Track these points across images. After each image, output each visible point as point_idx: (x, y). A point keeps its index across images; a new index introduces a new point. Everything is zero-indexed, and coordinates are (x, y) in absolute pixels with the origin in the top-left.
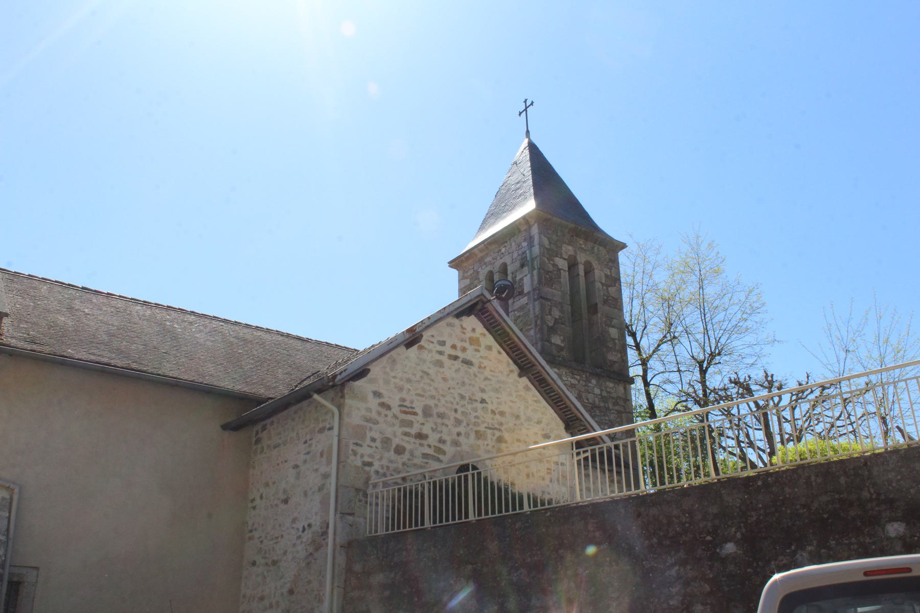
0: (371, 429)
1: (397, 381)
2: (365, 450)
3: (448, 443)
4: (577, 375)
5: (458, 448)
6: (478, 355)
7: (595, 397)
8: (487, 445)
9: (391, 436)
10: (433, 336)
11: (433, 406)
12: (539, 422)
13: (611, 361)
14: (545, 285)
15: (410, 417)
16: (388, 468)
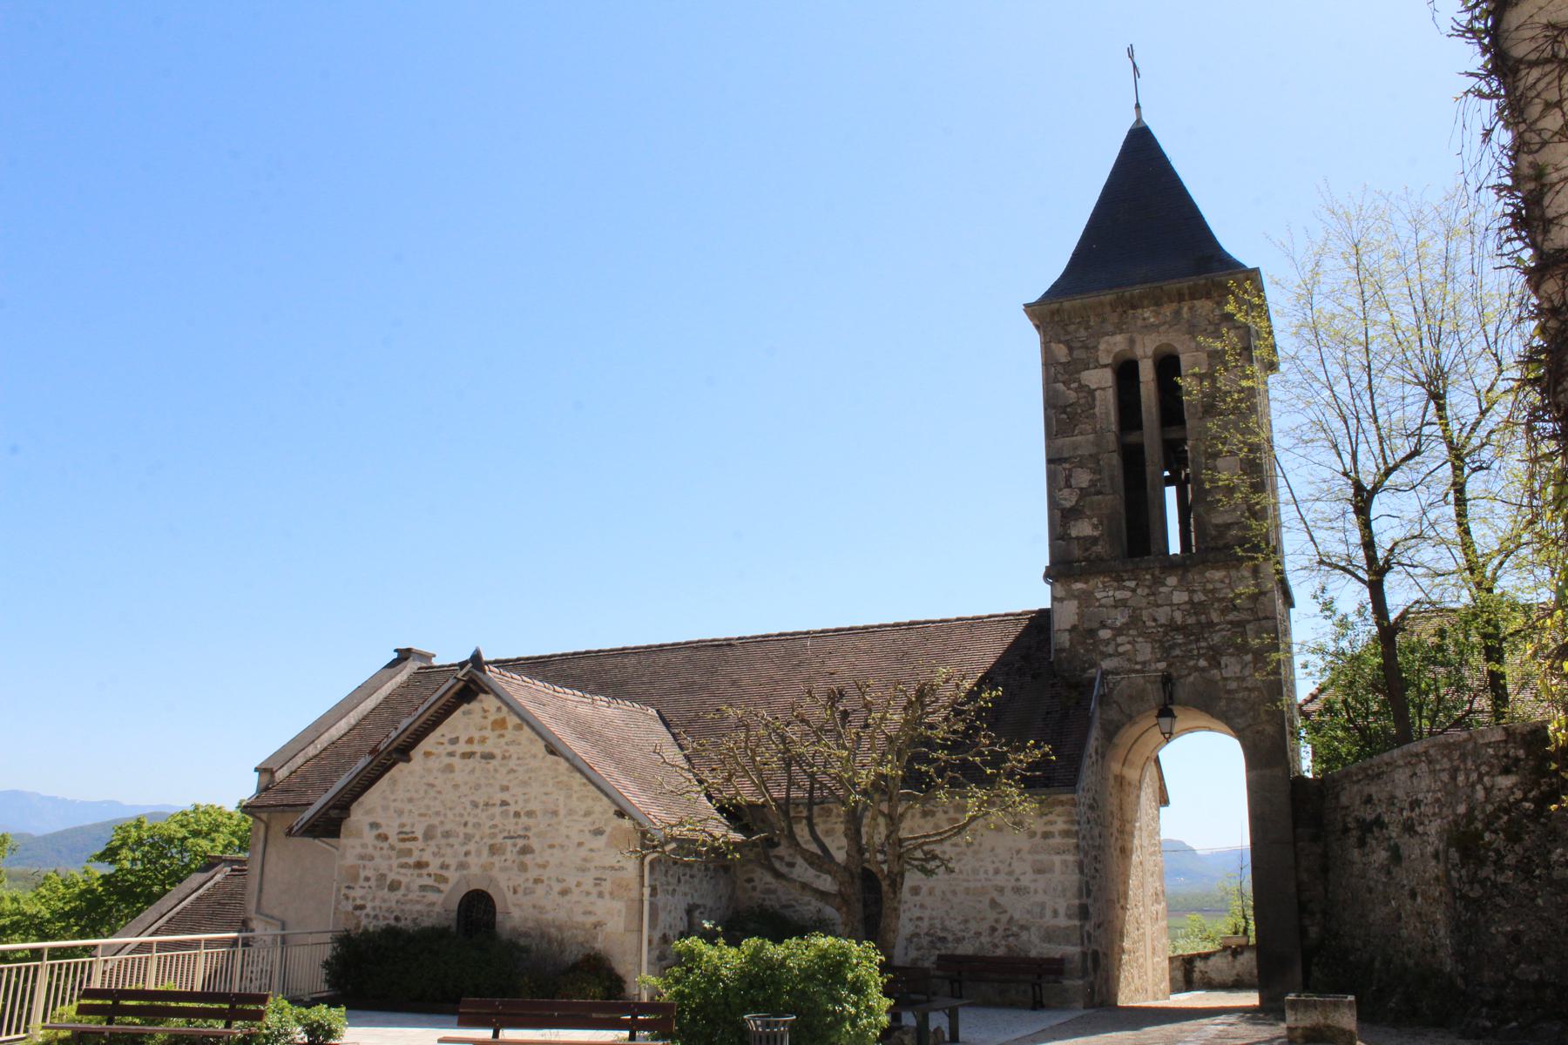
0: (364, 867)
1: (398, 804)
2: (357, 893)
3: (453, 868)
4: (1129, 580)
5: (465, 872)
6: (503, 741)
7: (1172, 611)
8: (505, 860)
10: (443, 736)
12: (587, 814)
13: (1217, 526)
15: (408, 845)
16: (380, 908)
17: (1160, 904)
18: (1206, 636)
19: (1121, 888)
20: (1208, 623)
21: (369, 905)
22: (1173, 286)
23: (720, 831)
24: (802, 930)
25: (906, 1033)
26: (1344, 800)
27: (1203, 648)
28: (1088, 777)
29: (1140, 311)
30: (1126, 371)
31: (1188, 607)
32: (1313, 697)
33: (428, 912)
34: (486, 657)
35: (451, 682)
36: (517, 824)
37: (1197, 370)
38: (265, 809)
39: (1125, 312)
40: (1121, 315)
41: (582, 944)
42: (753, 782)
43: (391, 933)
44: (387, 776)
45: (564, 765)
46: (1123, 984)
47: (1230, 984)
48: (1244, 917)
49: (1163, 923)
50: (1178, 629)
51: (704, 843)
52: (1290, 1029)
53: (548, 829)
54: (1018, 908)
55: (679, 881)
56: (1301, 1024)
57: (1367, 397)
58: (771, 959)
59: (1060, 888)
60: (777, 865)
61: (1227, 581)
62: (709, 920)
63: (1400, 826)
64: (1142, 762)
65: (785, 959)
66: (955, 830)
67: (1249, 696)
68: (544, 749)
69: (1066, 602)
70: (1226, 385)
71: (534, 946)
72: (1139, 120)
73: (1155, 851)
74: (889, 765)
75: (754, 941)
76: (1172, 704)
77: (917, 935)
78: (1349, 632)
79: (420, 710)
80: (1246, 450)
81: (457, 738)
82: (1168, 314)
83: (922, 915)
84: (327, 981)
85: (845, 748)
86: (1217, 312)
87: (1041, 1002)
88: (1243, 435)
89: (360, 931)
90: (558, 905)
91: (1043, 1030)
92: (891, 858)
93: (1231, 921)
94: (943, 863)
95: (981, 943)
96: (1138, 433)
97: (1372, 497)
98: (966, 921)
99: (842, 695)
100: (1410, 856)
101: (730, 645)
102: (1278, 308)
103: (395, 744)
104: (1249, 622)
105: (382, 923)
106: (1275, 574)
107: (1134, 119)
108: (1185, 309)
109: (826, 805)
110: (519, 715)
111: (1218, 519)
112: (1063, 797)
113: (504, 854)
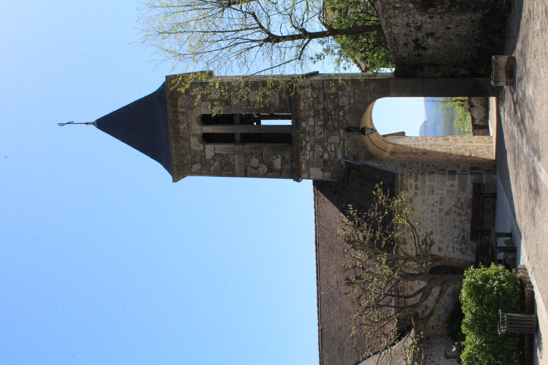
4: (302, 143)
7: (317, 125)
13: (280, 103)
14: (234, 172)
17: (449, 138)
18: (329, 111)
20: (323, 110)
22: (170, 115)
23: (409, 340)
24: (458, 304)
25: (507, 258)
26: (405, 55)
27: (335, 113)
28: (390, 168)
29: (180, 130)
30: (207, 138)
31: (316, 118)
32: (359, 66)
37: (209, 107)
39: (180, 137)
42: (387, 323)
46: (485, 157)
47: (486, 109)
48: (456, 101)
49: (458, 137)
51: (416, 349)
52: (507, 85)
54: (449, 203)
55: (433, 362)
56: (505, 80)
57: (227, 34)
58: (471, 320)
59: (441, 183)
60: (426, 314)
61: (305, 100)
62: (452, 348)
63: (418, 32)
64: (385, 143)
65: (472, 313)
66: (413, 229)
69: (311, 173)
70: (217, 95)
73: (425, 139)
74: (382, 259)
75: (463, 327)
76: (359, 128)
77: (461, 249)
78: (331, 48)
80: (247, 88)
82: (183, 118)
83: (452, 247)
85: (373, 279)
86: (184, 96)
87: (493, 194)
88: (240, 89)
91: (506, 194)
93: (457, 107)
94: (428, 236)
95: (465, 220)
96: (236, 135)
97: (272, 34)
98: (455, 226)
99: (348, 279)
100: (431, 29)
101: (321, 330)
102: (185, 69)
104: (324, 92)
106: (303, 79)
107: (92, 126)
108: (181, 110)
109: (399, 289)
111: (278, 103)
112: (399, 179)
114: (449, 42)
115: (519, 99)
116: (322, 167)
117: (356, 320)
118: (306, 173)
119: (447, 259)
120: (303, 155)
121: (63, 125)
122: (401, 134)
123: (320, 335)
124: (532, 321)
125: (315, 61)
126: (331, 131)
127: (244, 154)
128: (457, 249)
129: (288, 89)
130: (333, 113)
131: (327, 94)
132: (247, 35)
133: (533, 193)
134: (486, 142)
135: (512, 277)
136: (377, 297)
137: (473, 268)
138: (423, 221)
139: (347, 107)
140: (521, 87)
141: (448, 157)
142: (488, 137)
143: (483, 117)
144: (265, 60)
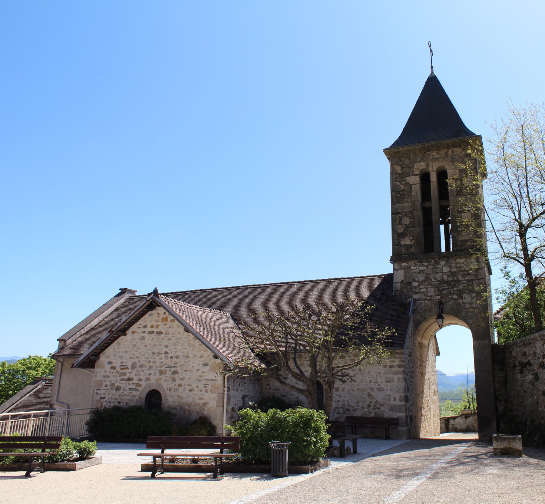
1: (121, 354)
2: (102, 392)
5: (149, 382)
6: (166, 326)
8: (166, 377)
9: (115, 382)
10: (140, 324)
11: (137, 362)
12: (201, 357)
15: (124, 371)
16: (112, 398)
17: (436, 396)
18: (457, 285)
19: (421, 389)
20: (458, 280)
21: (107, 397)
22: (444, 142)
23: (257, 363)
25: (335, 449)
26: (514, 354)
27: (455, 290)
28: (408, 342)
29: (431, 152)
30: (425, 177)
31: (449, 274)
32: (498, 312)
33: (133, 400)
34: (160, 292)
35: (144, 302)
36: (171, 361)
37: (455, 177)
38: (61, 357)
39: (425, 153)
40: (424, 154)
41: (198, 412)
43: (116, 409)
44: (116, 342)
45: (192, 336)
46: (422, 429)
47: (464, 430)
48: (469, 402)
49: (438, 404)
50: (445, 282)
52: (494, 449)
53: (185, 363)
54: (379, 397)
55: (239, 385)
56: (499, 447)
57: (525, 189)
58: (280, 418)
59: (397, 389)
62: (251, 402)
63: (538, 365)
64: (429, 338)
65: (286, 418)
66: (356, 364)
67: (474, 310)
68: (183, 330)
69: (399, 271)
70: (467, 183)
71: (178, 413)
72: (432, 73)
73: (434, 374)
74: (329, 336)
75: (273, 410)
76: (442, 313)
77: (338, 408)
78: (516, 285)
79: (131, 314)
80: (474, 210)
81: (147, 325)
82: (443, 154)
83: (340, 400)
84: (87, 430)
85: (309, 329)
86: (463, 153)
87: (389, 436)
88: (474, 203)
89: (103, 408)
90: (188, 395)
91: (391, 448)
92: (329, 375)
93: (463, 404)
94: (350, 378)
95: (364, 412)
96: (429, 202)
97: (527, 230)
98: (358, 402)
99: (309, 307)
100: (542, 378)
101: (261, 287)
102: (488, 151)
103: (120, 328)
104: (474, 280)
105: (112, 405)
106: (485, 261)
107: (430, 73)
108: (450, 152)
109: (300, 353)
110: (173, 316)
111: (462, 238)
112: (398, 351)
113: (165, 374)
114: (530, 395)
115: (481, 460)
116: (405, 281)
117: (273, 316)
118: (398, 267)
119: (331, 395)
120: (414, 263)
121: (429, 46)
122: (437, 352)
123: (256, 286)
124: (282, 472)
125: (503, 271)
126: (438, 287)
127: (413, 211)
128: (337, 404)
129: (475, 247)
130: (455, 289)
131: (473, 282)
132: (526, 207)
133: (397, 472)
134: (435, 430)
135: (319, 454)
136: (294, 333)
137: (326, 418)
138: (362, 374)
139: (462, 301)
140: (495, 463)
141: (420, 395)
142: (439, 431)
143: (456, 427)
144: (502, 225)
